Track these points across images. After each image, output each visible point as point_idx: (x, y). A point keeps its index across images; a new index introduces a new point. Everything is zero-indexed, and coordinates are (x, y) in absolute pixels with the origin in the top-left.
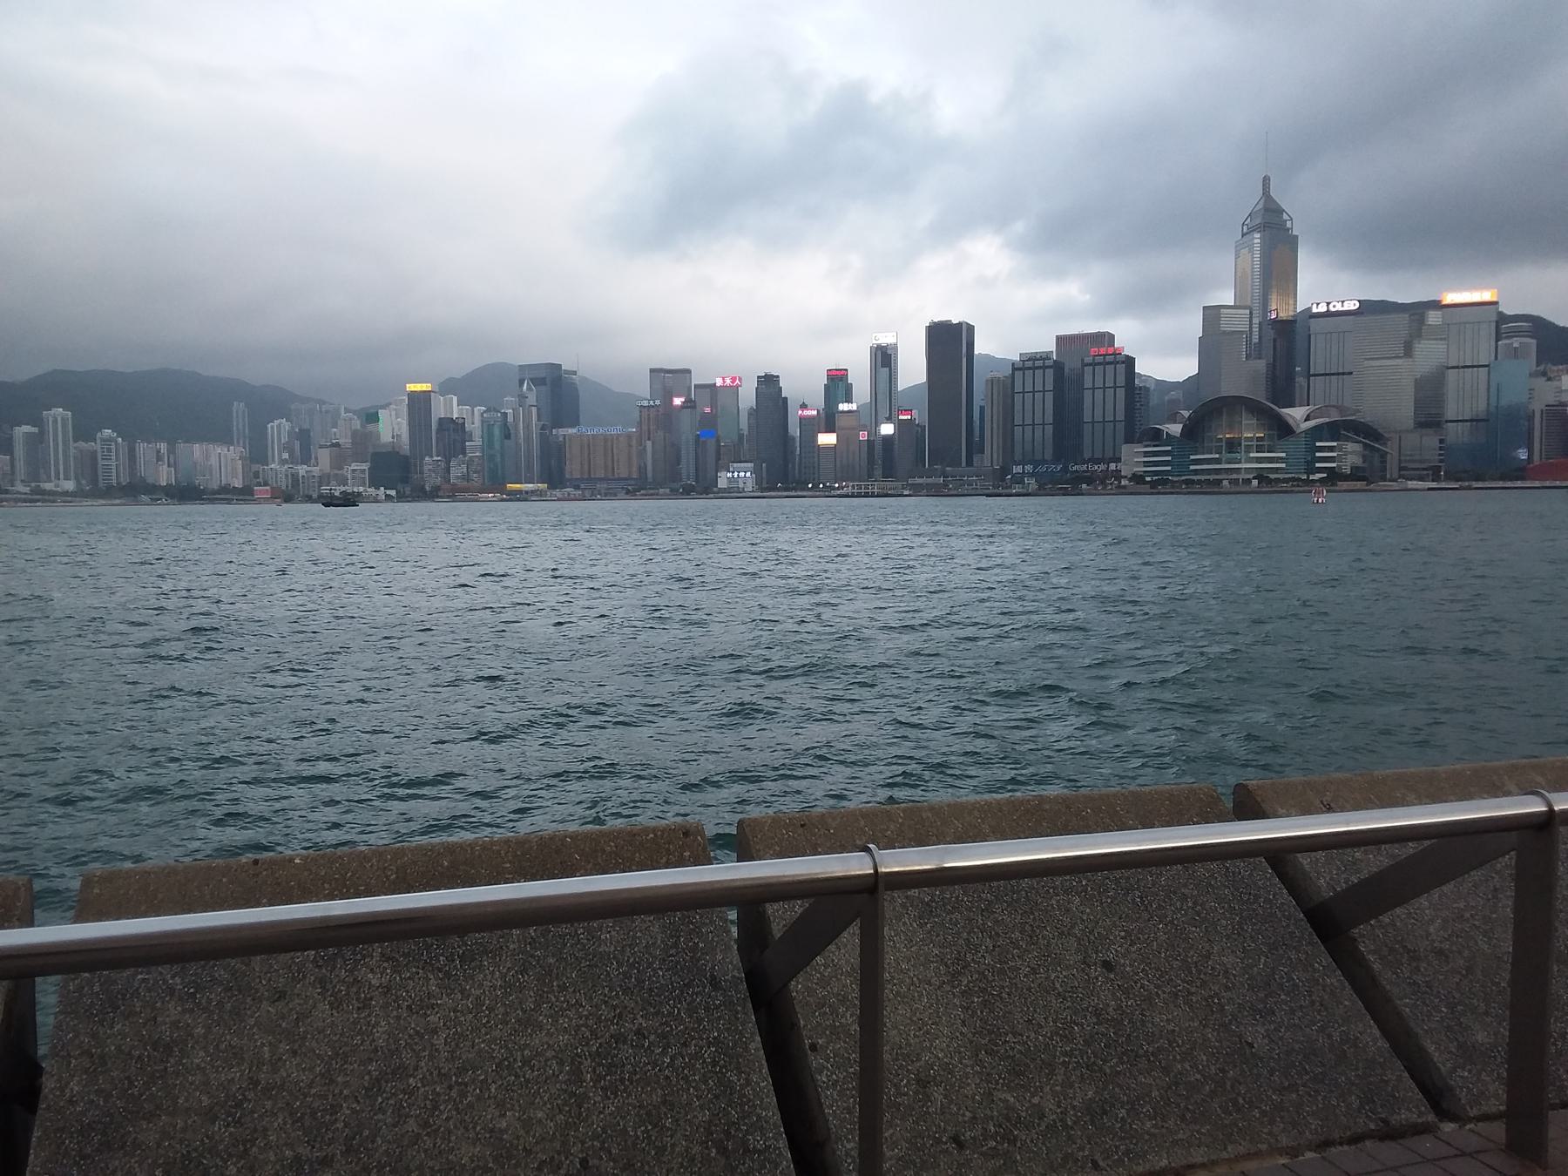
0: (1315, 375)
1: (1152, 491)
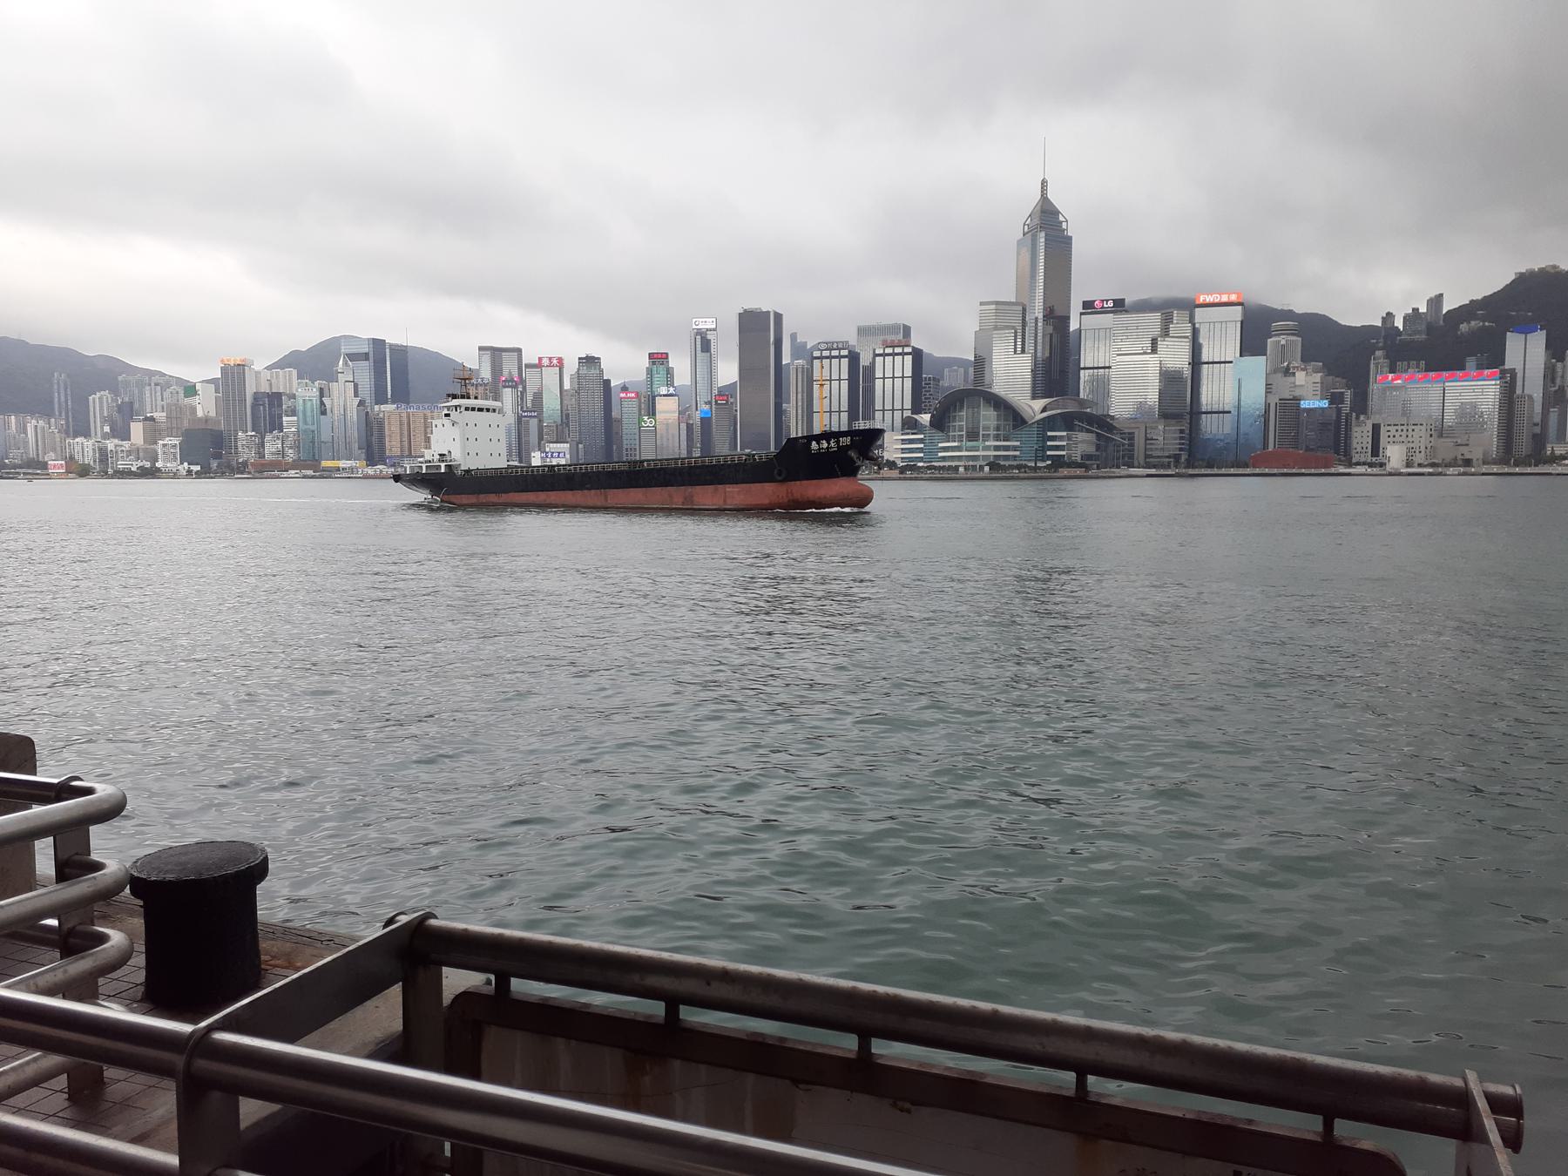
0: (1085, 368)
1: (901, 476)
